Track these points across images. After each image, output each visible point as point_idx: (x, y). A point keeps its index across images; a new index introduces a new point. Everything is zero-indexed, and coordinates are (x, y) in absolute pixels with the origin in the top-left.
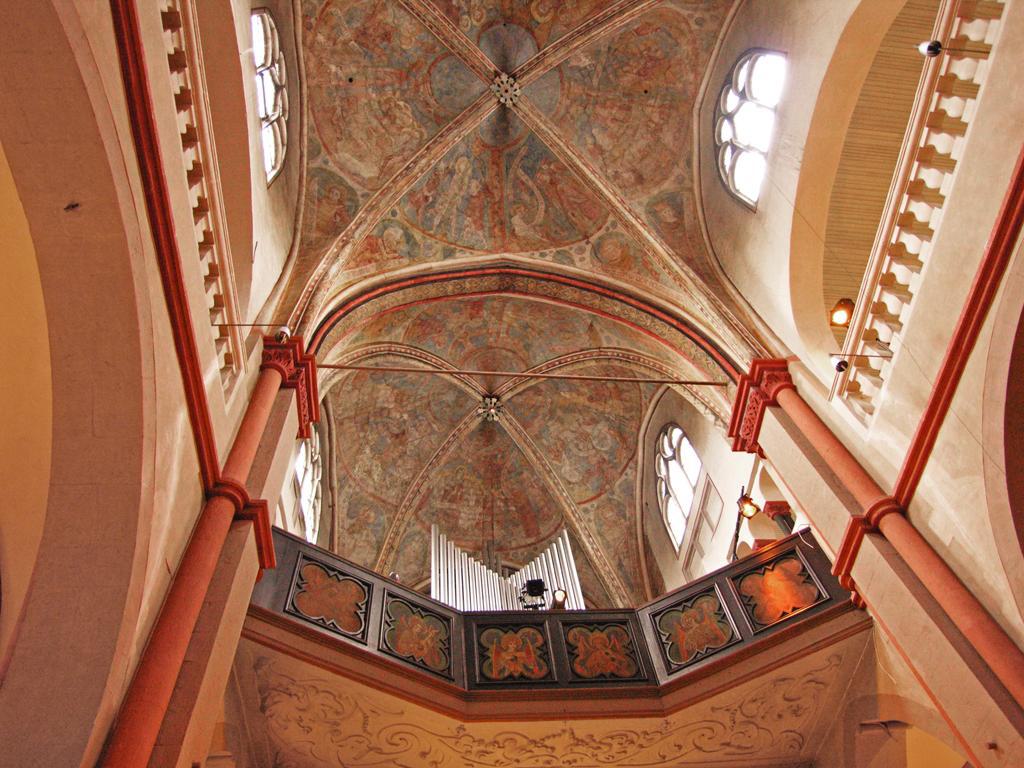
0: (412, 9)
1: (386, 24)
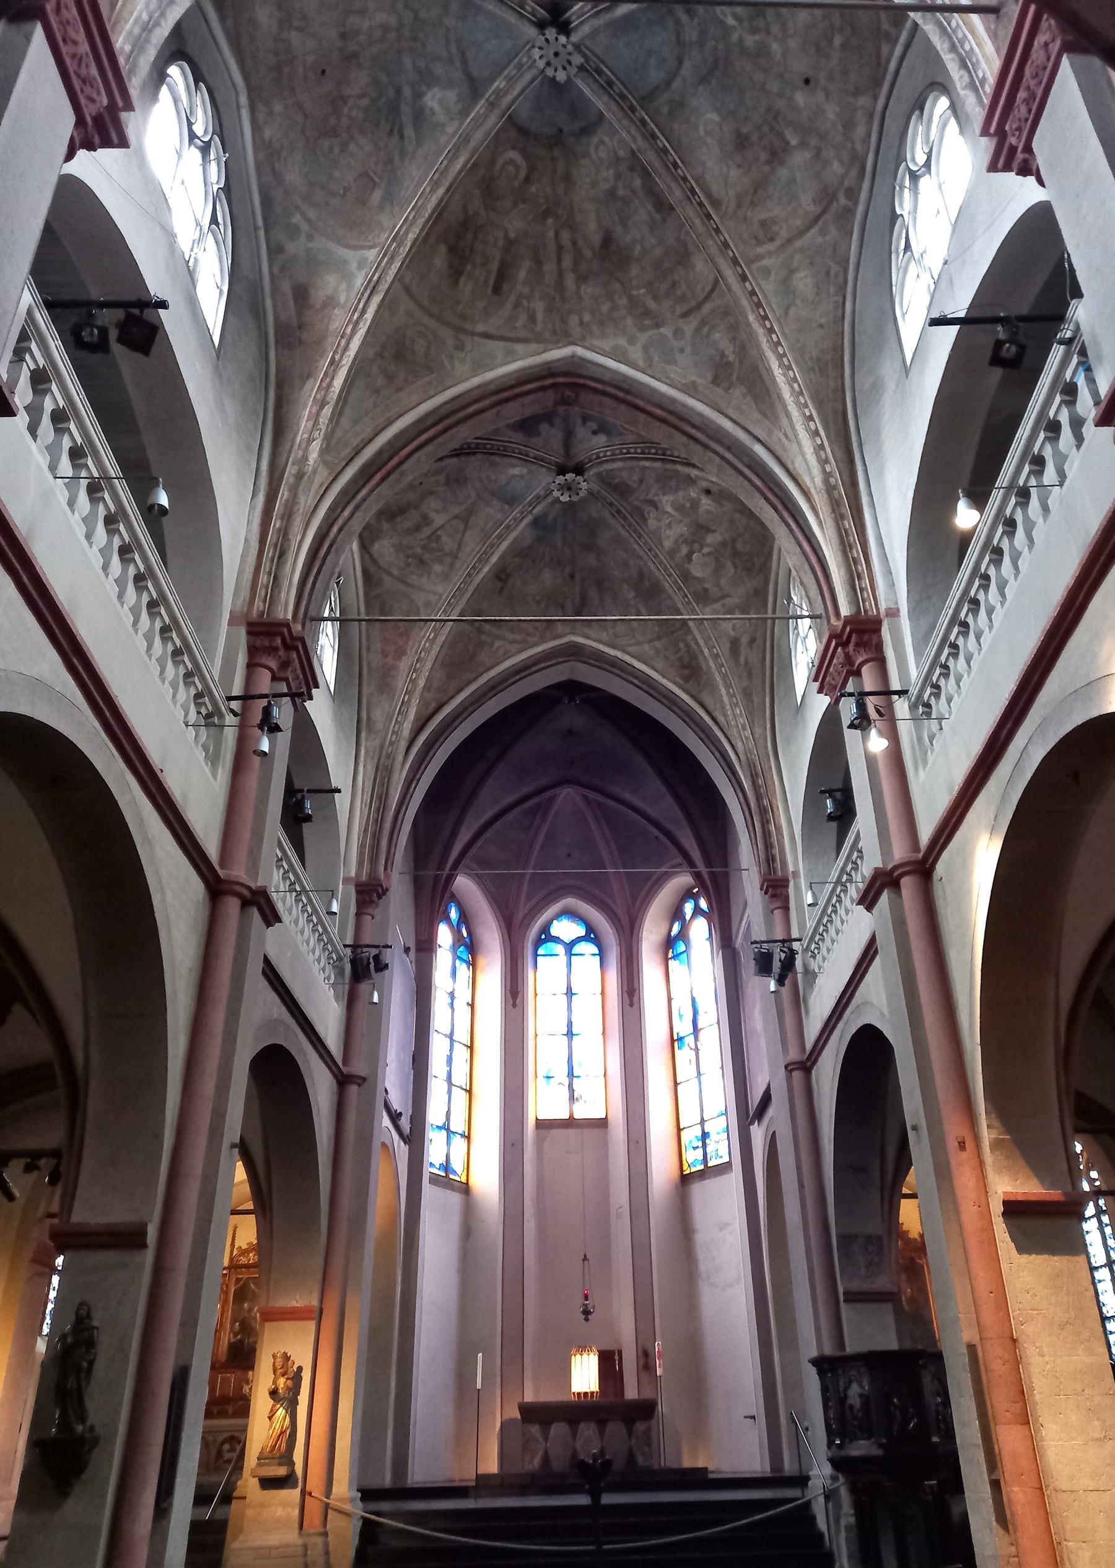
0: (701, 204)
1: (739, 166)
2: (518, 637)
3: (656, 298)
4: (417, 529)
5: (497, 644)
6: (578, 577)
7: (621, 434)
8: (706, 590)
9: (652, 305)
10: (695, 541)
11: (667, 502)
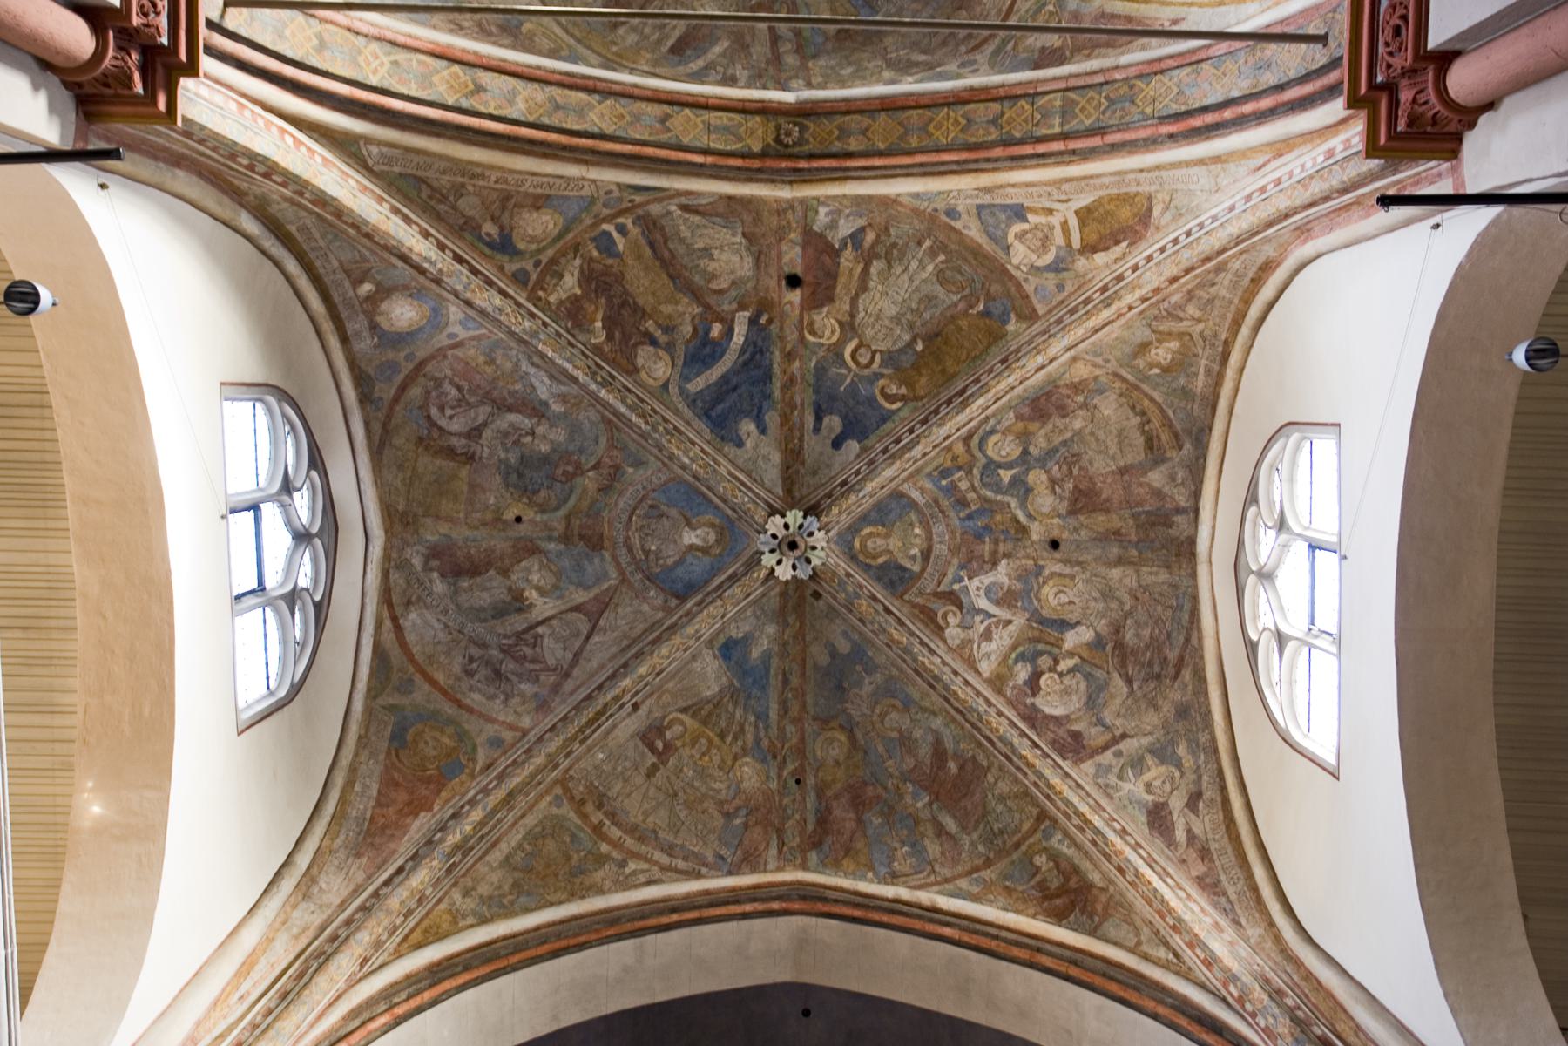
2: (681, 864)
3: (924, 52)
4: (500, 612)
5: (632, 866)
6: (811, 781)
7: (885, 417)
8: (1076, 736)
9: (922, 58)
10: (1041, 653)
11: (976, 589)
